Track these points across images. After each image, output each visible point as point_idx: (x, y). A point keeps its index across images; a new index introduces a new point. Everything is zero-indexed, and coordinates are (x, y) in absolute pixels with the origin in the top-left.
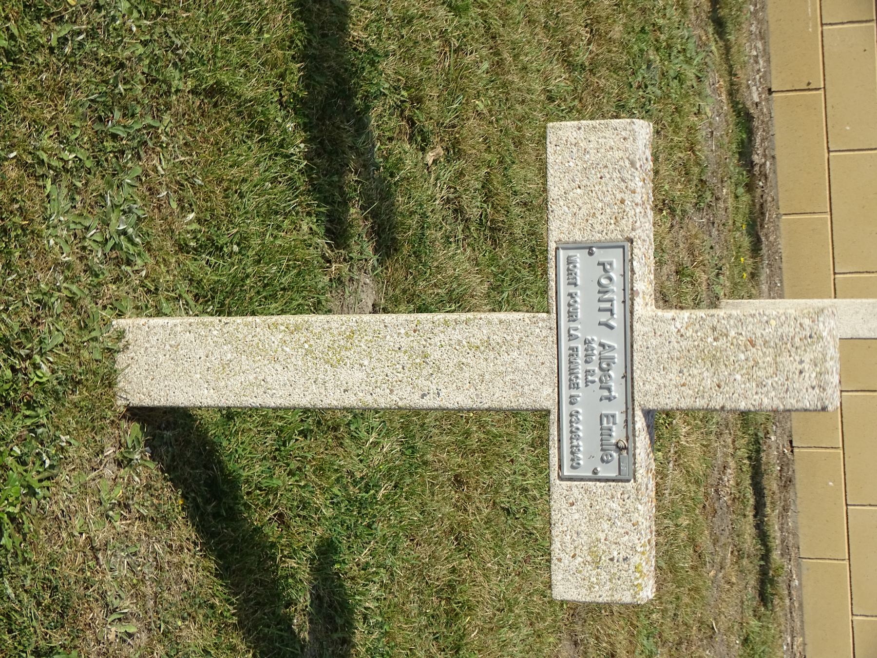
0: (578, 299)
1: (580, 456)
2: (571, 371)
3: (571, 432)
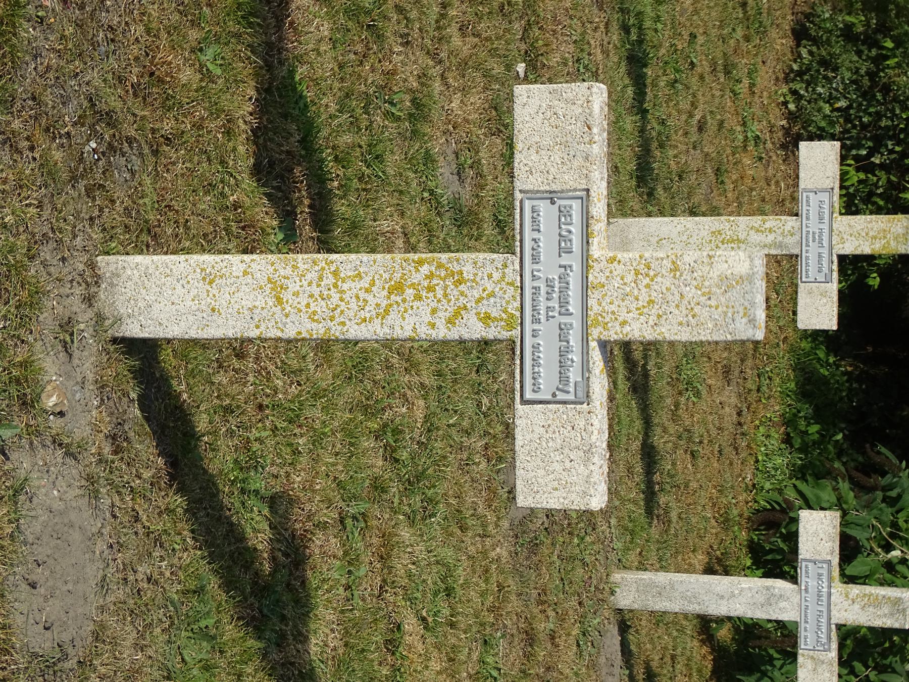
0: (541, 244)
1: (541, 381)
2: (534, 308)
3: (533, 360)
